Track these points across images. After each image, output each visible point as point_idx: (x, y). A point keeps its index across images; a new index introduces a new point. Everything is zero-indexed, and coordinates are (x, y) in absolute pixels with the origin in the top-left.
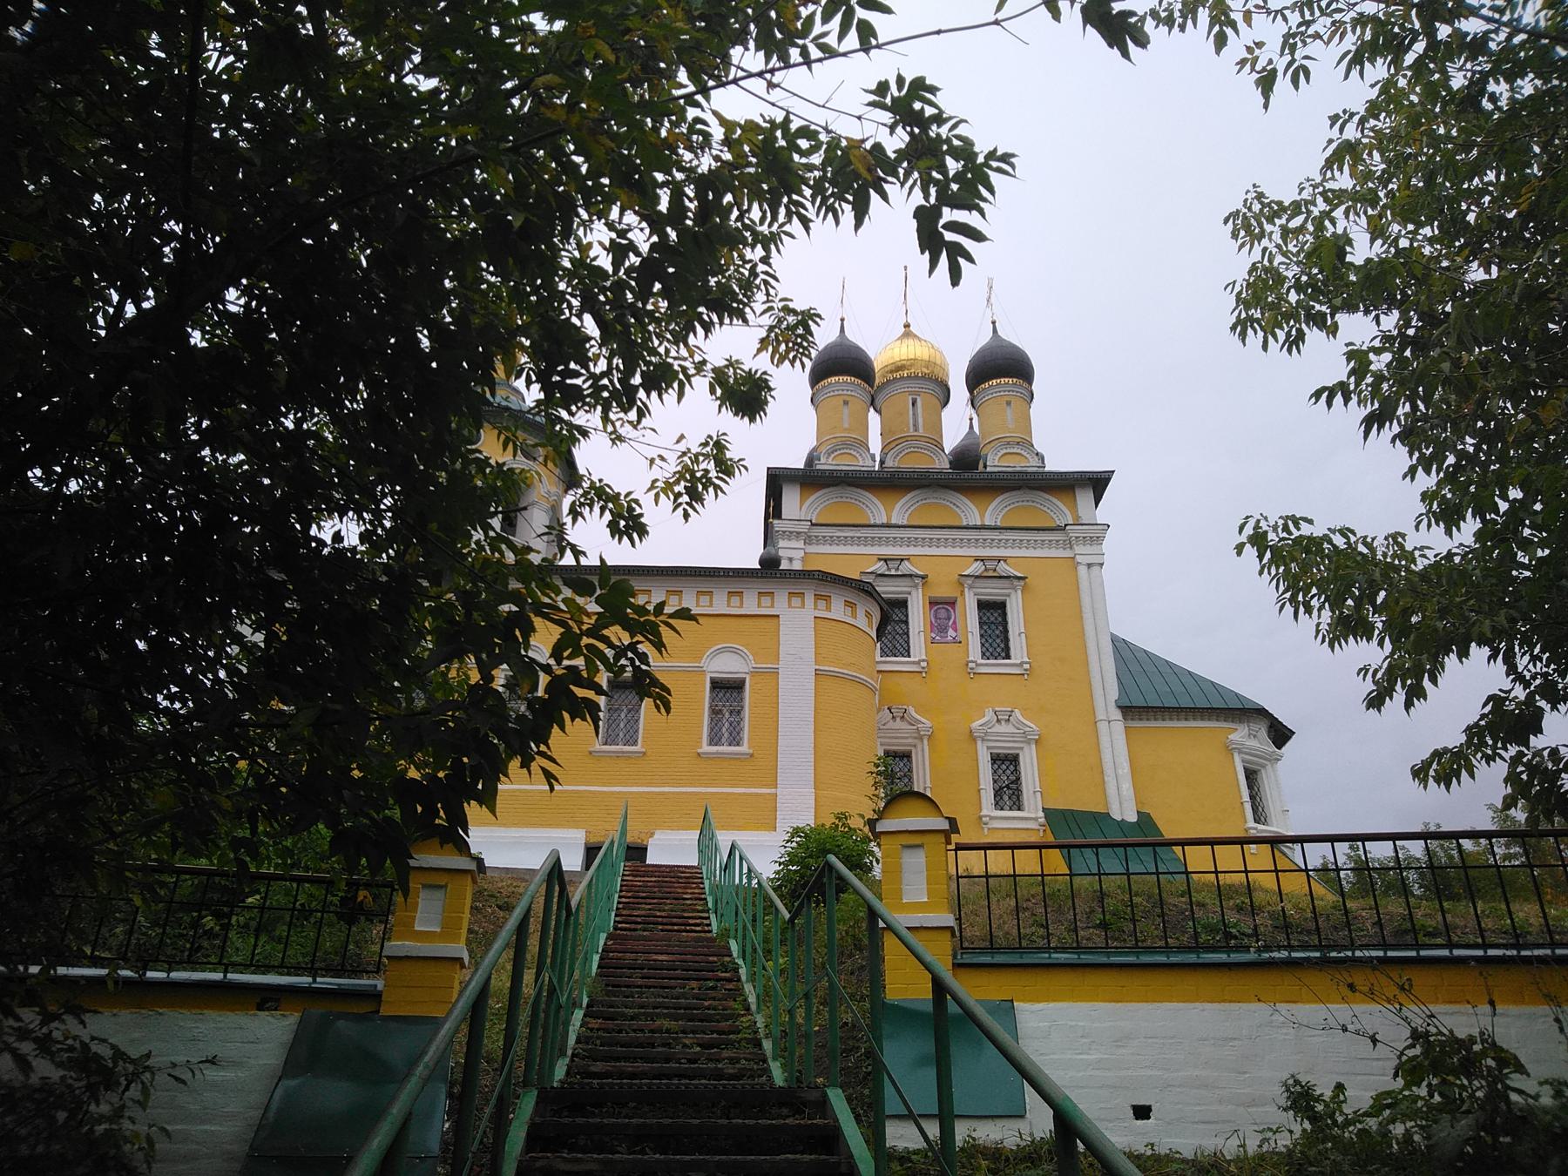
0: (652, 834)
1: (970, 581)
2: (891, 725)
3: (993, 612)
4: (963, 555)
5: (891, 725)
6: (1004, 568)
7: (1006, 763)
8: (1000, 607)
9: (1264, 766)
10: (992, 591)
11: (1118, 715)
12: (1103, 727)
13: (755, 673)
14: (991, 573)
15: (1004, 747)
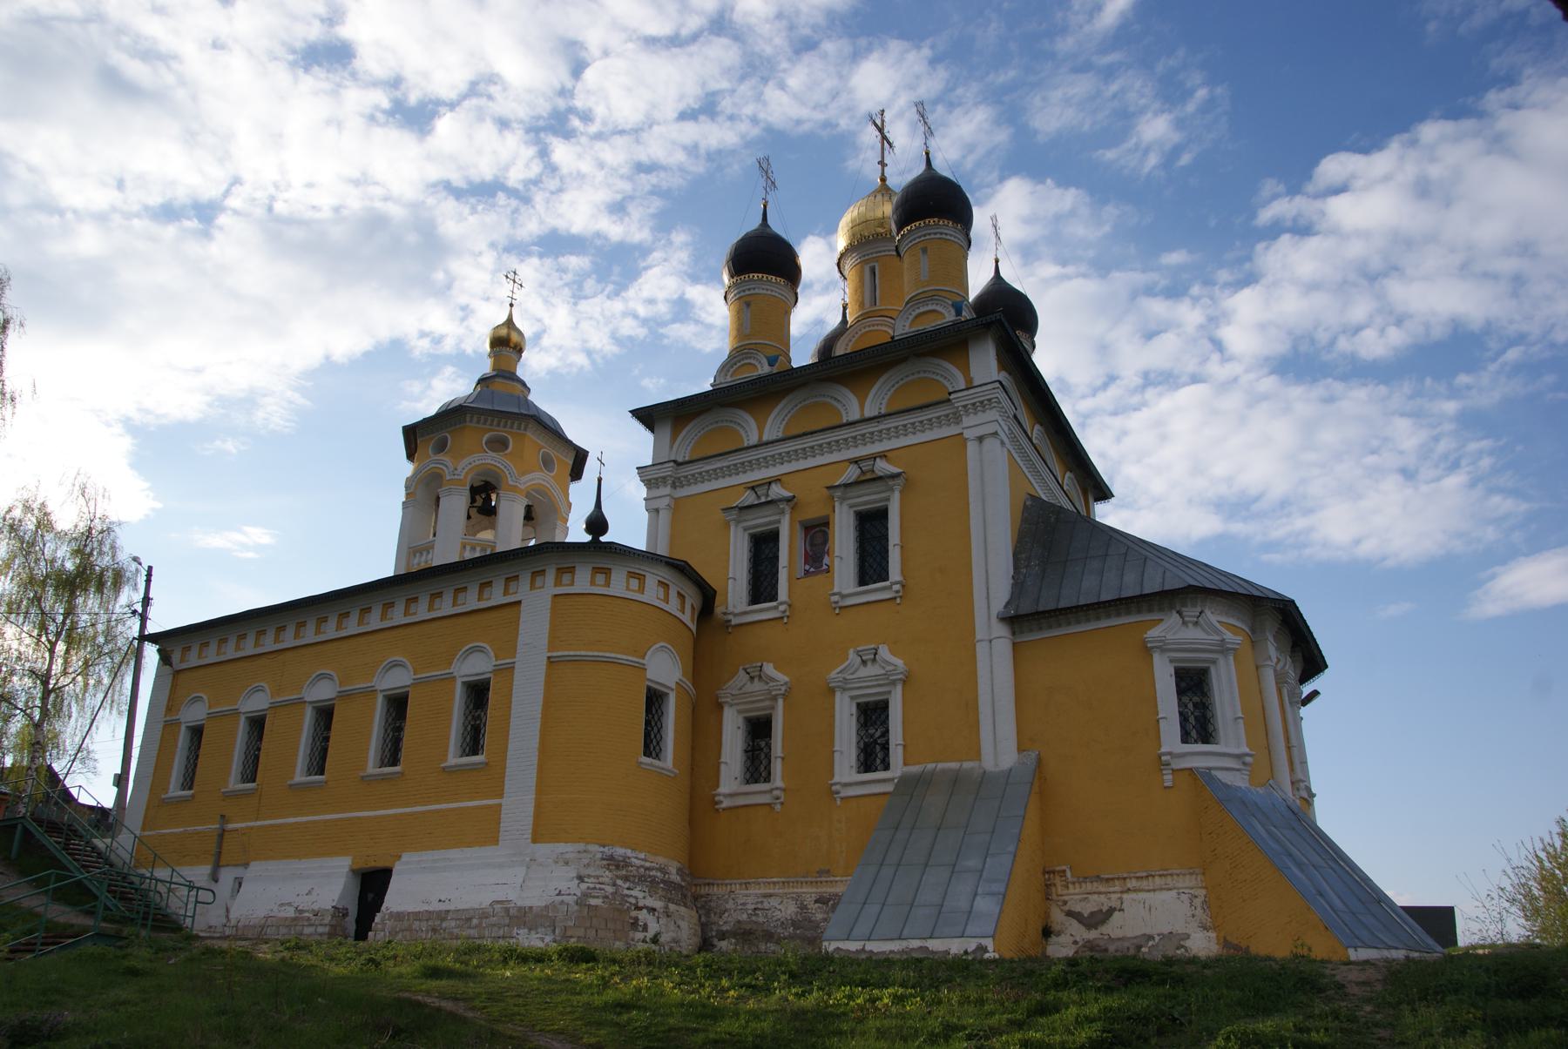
0: (400, 857)
1: (838, 493)
2: (750, 687)
3: (871, 526)
4: (835, 459)
5: (750, 687)
6: (883, 467)
7: (873, 714)
8: (881, 515)
9: (1214, 662)
10: (868, 498)
11: (1001, 630)
12: (981, 650)
13: (498, 670)
14: (868, 476)
15: (871, 693)
